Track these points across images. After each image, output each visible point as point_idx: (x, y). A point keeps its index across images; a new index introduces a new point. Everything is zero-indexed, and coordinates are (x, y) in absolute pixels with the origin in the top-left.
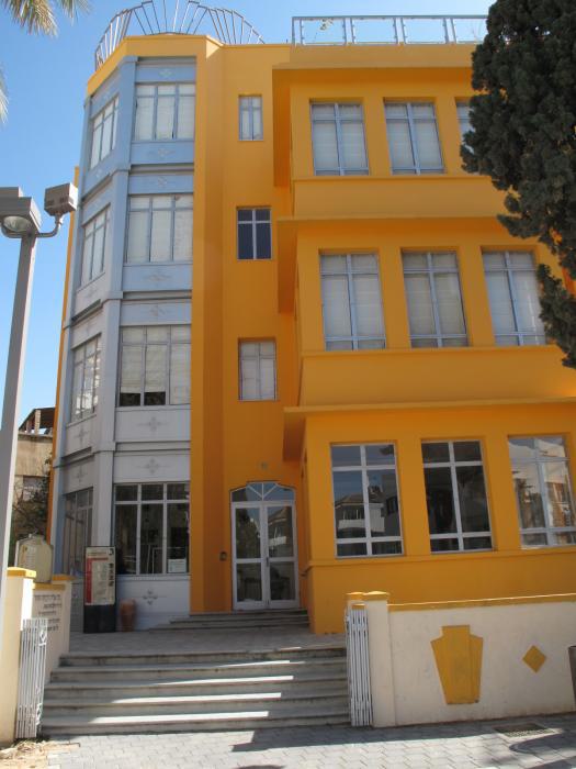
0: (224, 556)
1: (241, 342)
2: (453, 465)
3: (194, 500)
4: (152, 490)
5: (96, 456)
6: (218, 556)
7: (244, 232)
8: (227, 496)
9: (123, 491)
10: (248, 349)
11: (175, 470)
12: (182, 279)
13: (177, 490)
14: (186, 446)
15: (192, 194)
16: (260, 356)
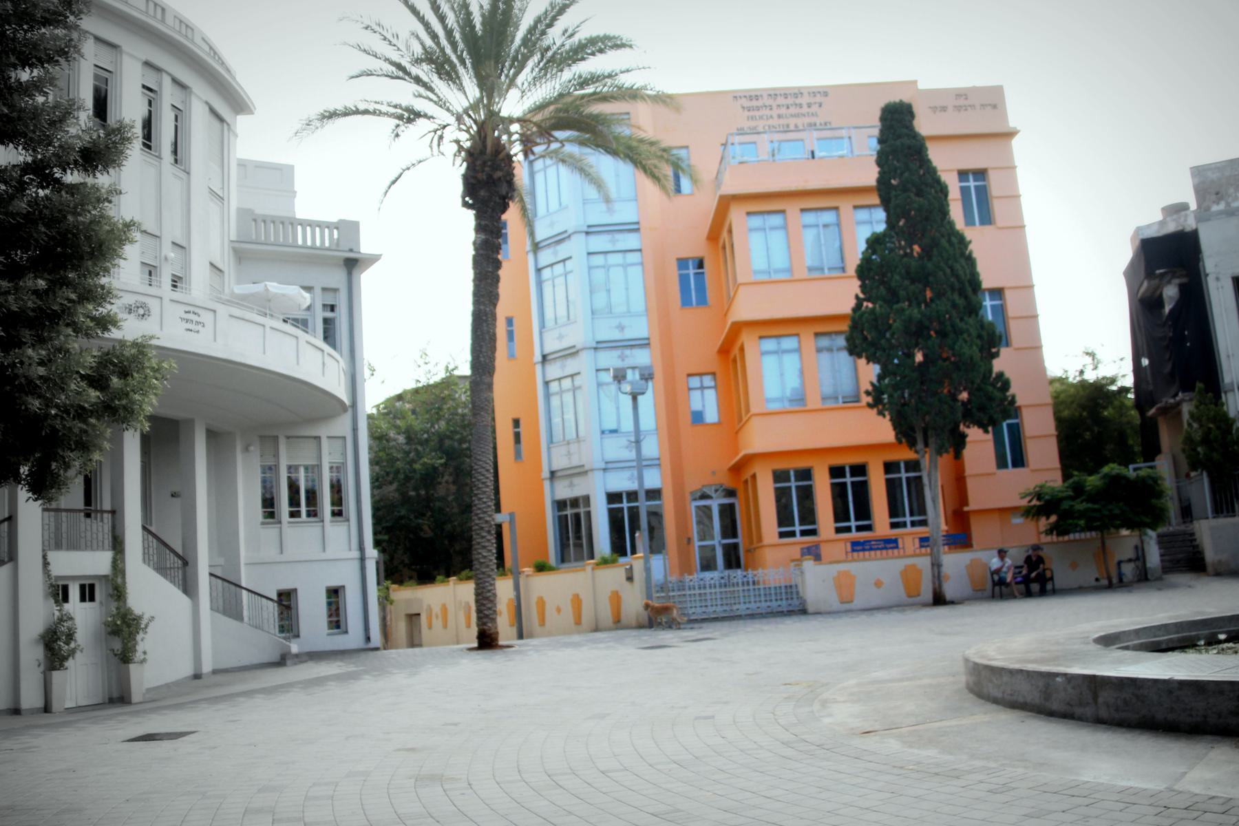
0: (689, 540)
1: (689, 375)
2: (848, 480)
3: (668, 505)
4: (632, 496)
5: (590, 474)
6: (685, 541)
7: (684, 280)
8: (688, 497)
9: (613, 497)
10: (695, 382)
11: (653, 479)
12: (639, 328)
13: (654, 494)
14: (656, 462)
15: (640, 250)
16: (702, 388)
